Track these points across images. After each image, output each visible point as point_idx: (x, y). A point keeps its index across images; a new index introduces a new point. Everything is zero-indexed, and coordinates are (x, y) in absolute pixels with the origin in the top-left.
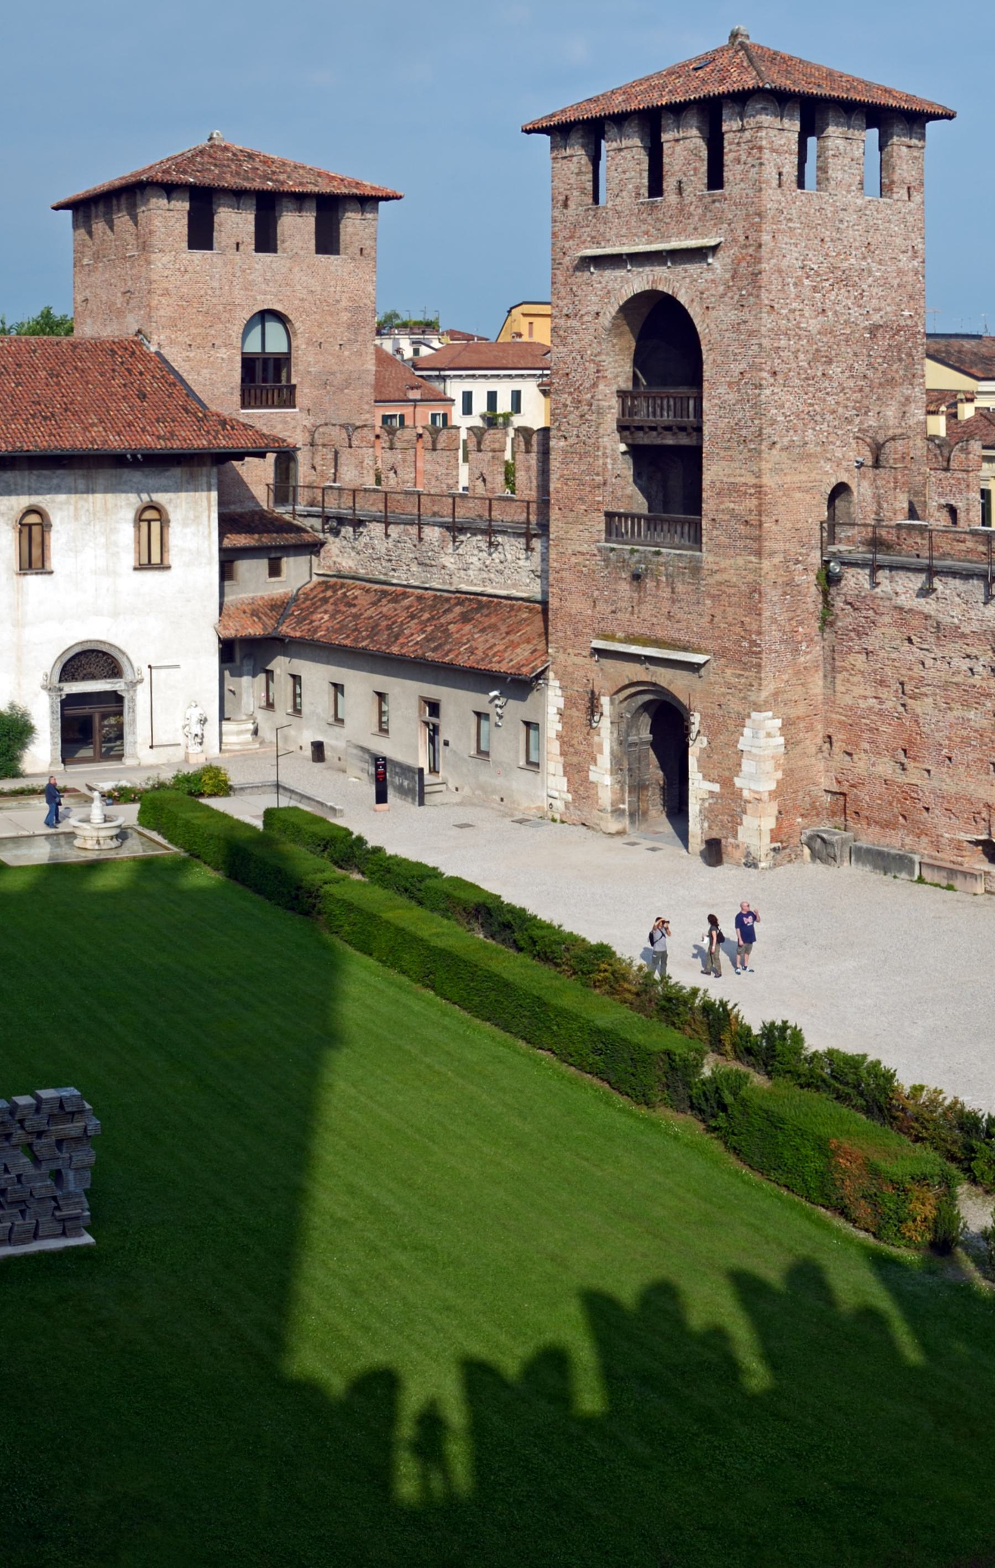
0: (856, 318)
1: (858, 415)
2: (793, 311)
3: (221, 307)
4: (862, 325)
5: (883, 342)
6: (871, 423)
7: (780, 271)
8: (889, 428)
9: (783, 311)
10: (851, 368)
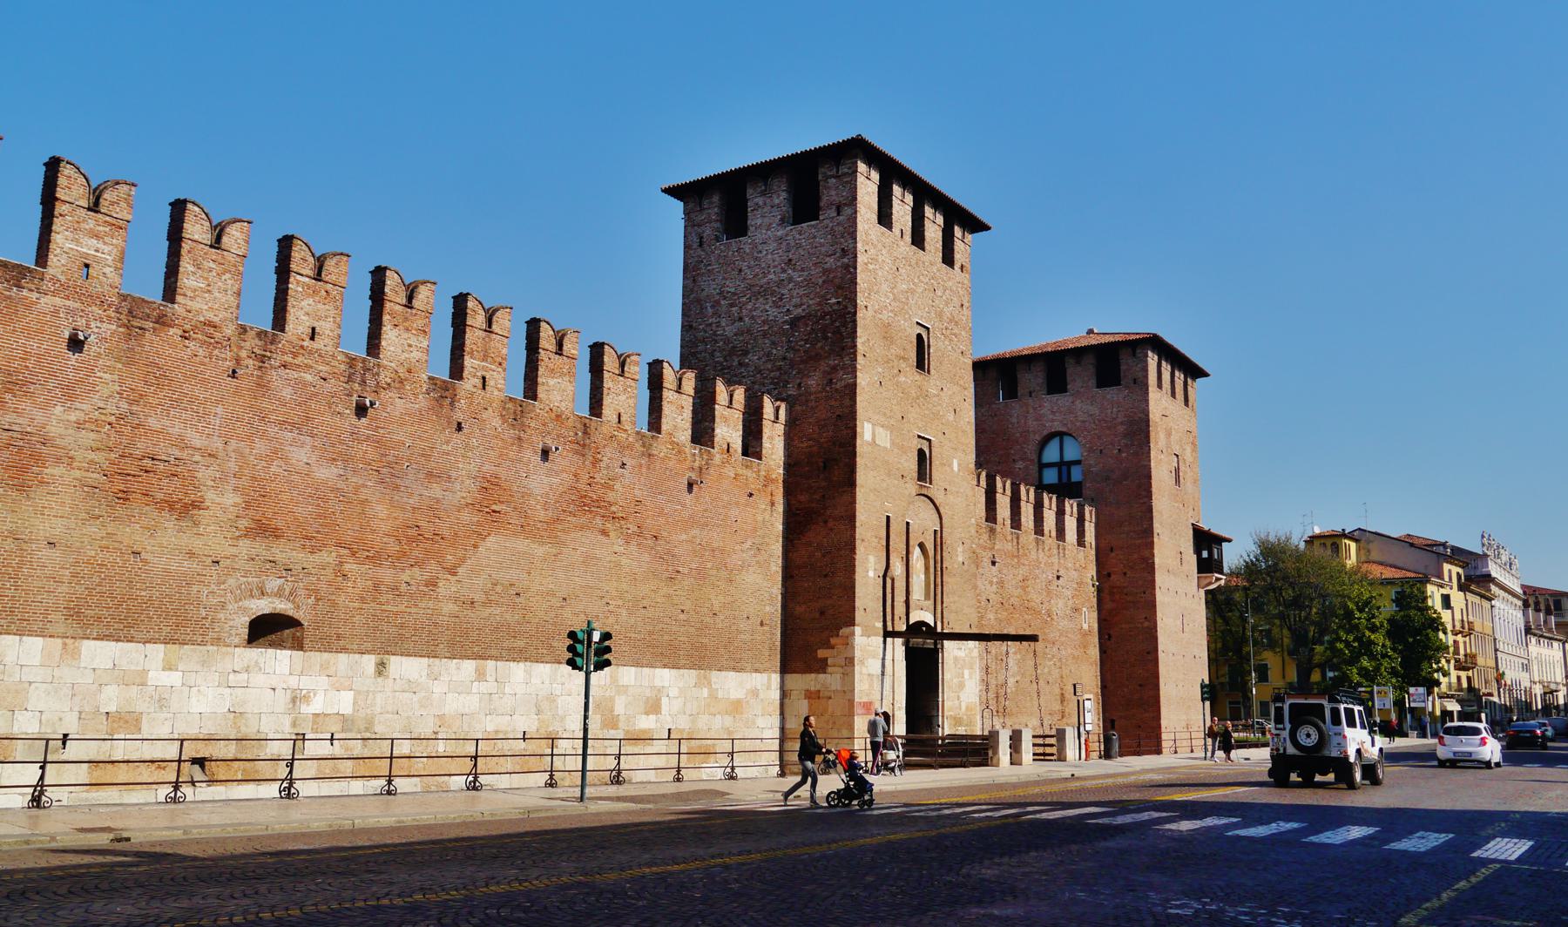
0: (776, 317)
1: (775, 389)
2: (711, 324)
3: (1018, 435)
4: (781, 321)
6: (790, 393)
8: (810, 394)
9: (701, 327)
10: (769, 354)
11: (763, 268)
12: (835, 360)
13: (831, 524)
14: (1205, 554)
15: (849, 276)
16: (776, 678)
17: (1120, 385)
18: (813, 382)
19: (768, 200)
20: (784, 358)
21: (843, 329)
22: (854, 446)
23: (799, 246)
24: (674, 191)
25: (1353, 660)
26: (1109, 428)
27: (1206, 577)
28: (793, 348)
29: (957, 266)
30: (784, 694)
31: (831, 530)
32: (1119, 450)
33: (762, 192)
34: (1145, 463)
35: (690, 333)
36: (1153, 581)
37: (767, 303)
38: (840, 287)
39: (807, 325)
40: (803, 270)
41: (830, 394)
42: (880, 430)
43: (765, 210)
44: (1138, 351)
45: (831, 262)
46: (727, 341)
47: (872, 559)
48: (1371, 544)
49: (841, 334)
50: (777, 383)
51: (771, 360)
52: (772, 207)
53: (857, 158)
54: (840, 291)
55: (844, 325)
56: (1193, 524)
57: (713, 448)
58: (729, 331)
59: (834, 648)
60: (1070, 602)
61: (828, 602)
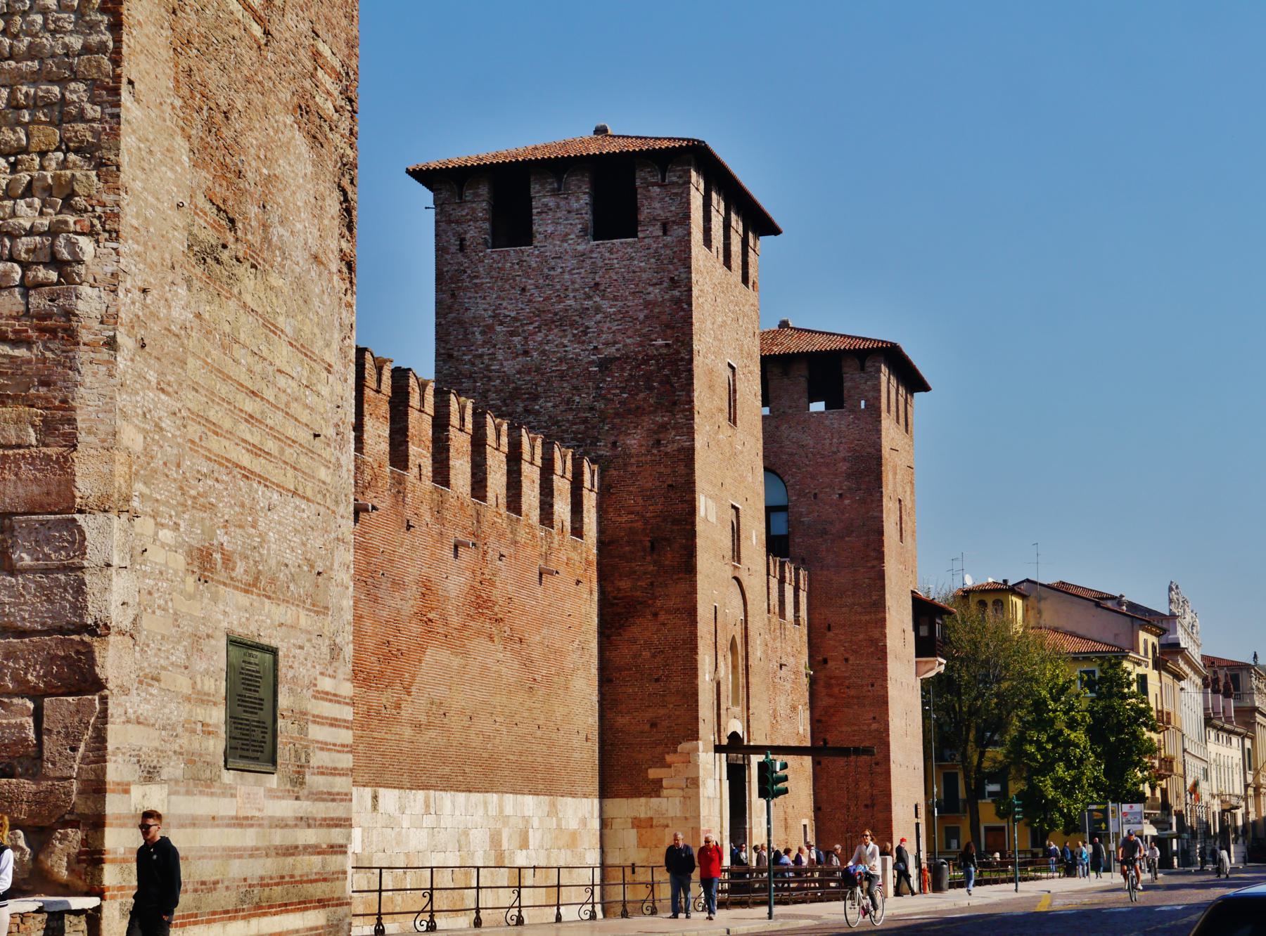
2: (481, 356)
4: (586, 360)
5: (617, 376)
7: (461, 323)
8: (630, 456)
10: (569, 402)
11: (558, 290)
12: (663, 416)
13: (662, 617)
14: (924, 631)
15: (682, 313)
16: (596, 801)
17: (842, 407)
18: (634, 441)
19: (562, 203)
20: (592, 409)
21: (674, 379)
22: (693, 524)
23: (611, 268)
24: (424, 176)
25: (1047, 768)
26: (827, 465)
27: (926, 662)
28: (604, 397)
29: (751, 284)
30: (604, 824)
31: (664, 624)
32: (841, 495)
33: (553, 190)
34: (875, 514)
35: (450, 364)
36: (885, 670)
37: (566, 336)
38: (667, 326)
39: (623, 370)
40: (615, 298)
41: (658, 458)
42: (710, 502)
43: (559, 215)
44: (868, 364)
45: (655, 293)
46: (506, 379)
47: (707, 657)
48: (1042, 602)
49: (672, 386)
50: (583, 440)
51: (571, 409)
52: (569, 212)
53: (690, 165)
54: (669, 331)
55: (677, 373)
56: (913, 592)
57: (552, 528)
58: (510, 367)
59: (670, 766)
60: (790, 698)
61: (662, 712)
